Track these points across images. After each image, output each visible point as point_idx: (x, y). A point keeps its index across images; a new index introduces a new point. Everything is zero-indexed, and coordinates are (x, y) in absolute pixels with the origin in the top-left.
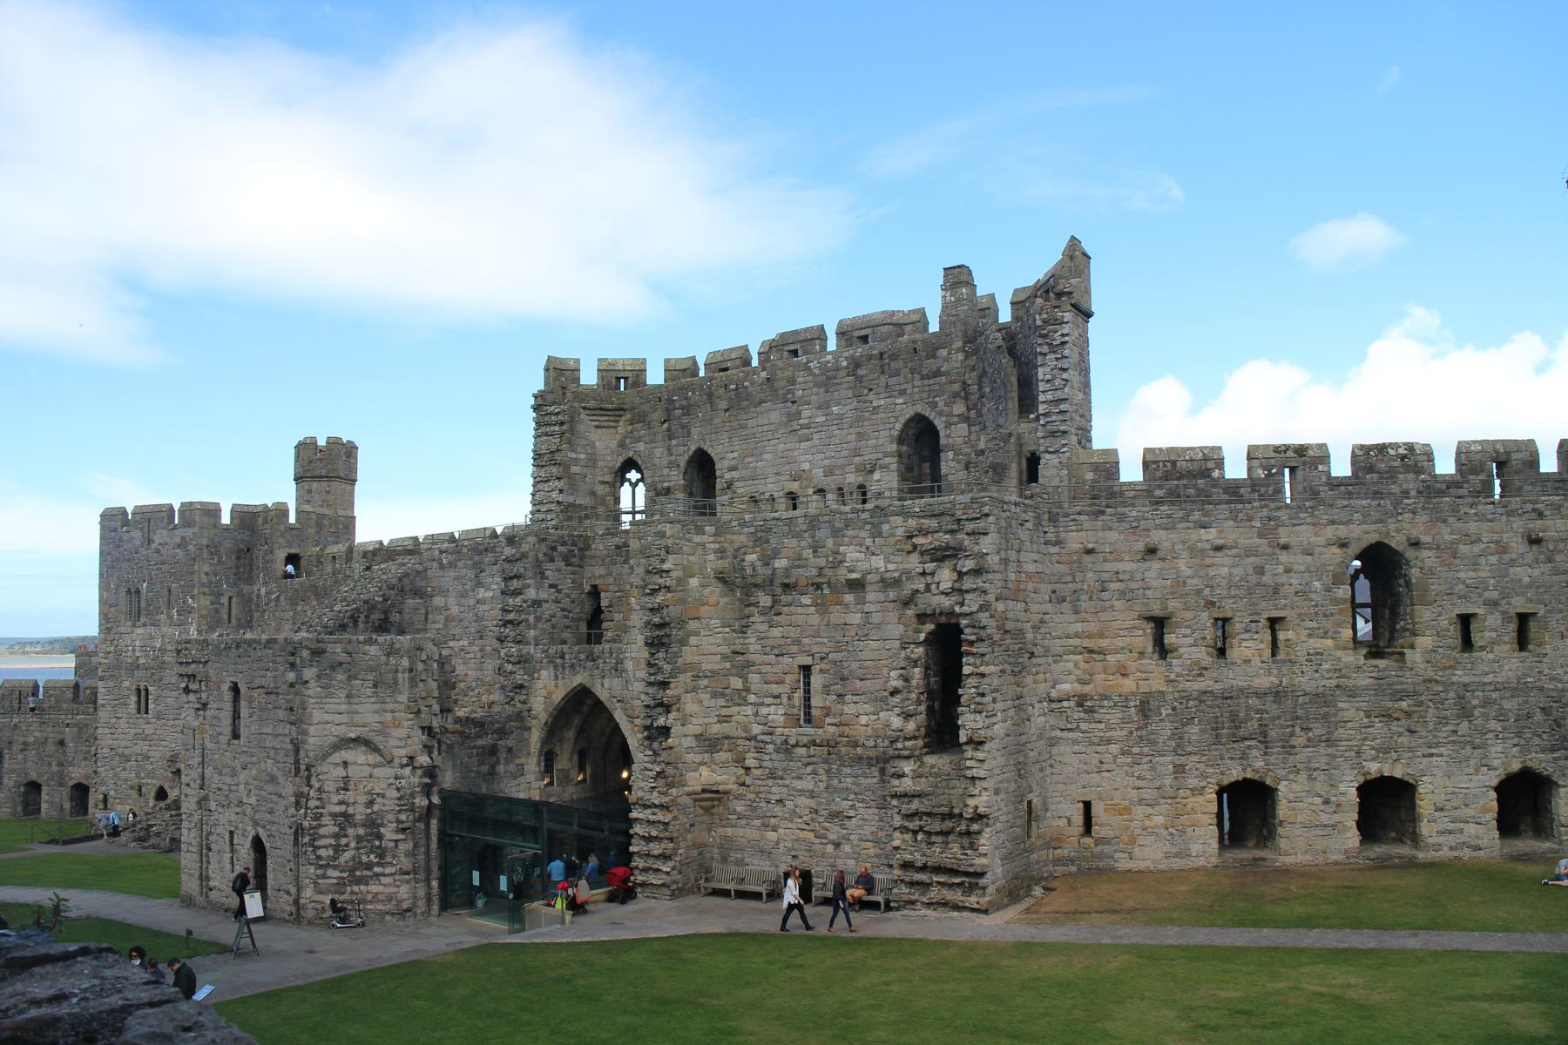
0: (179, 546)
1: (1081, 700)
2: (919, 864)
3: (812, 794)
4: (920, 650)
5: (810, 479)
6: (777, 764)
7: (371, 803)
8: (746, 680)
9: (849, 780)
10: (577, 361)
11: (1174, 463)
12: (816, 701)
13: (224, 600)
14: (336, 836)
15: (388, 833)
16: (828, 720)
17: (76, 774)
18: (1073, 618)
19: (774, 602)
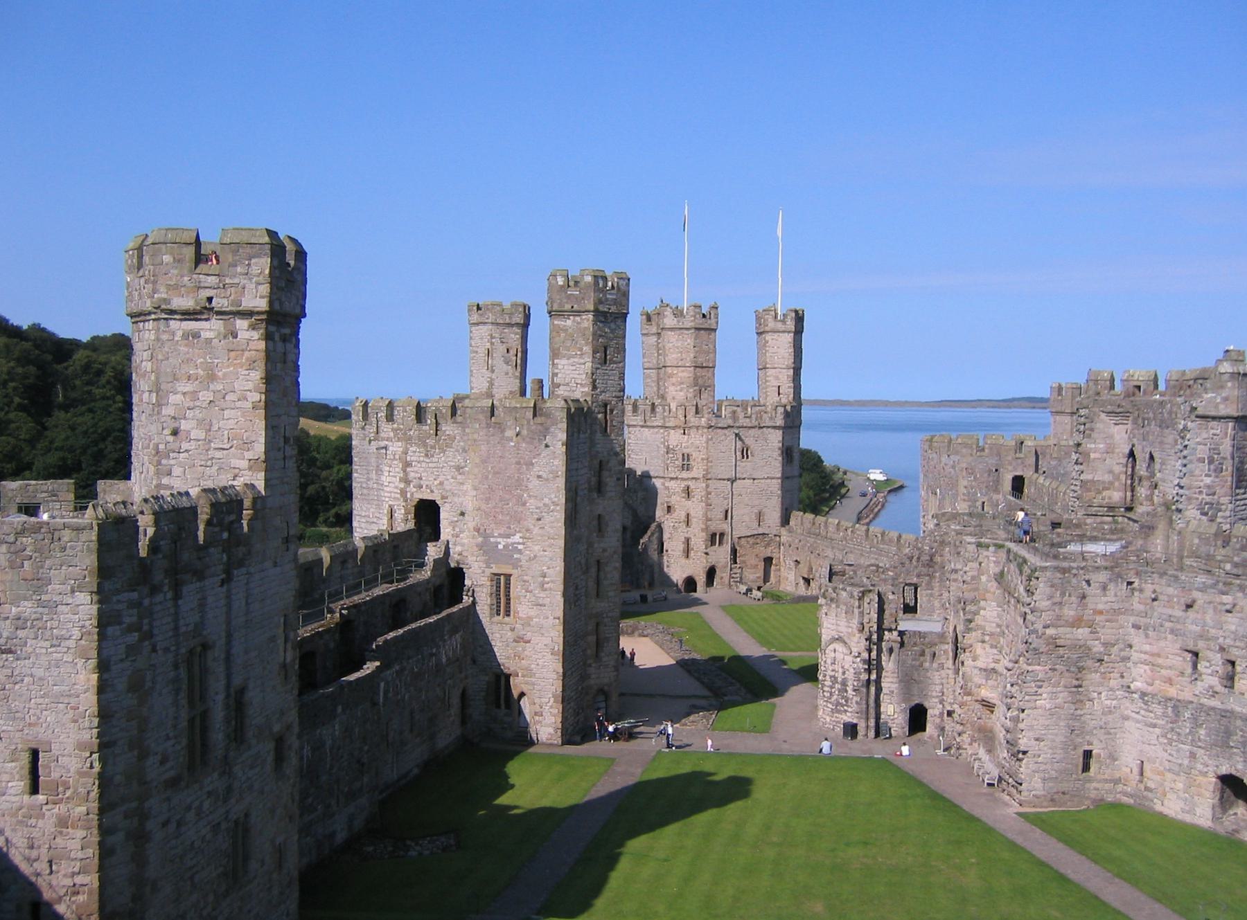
1: (1144, 694)
7: (844, 673)
14: (831, 687)
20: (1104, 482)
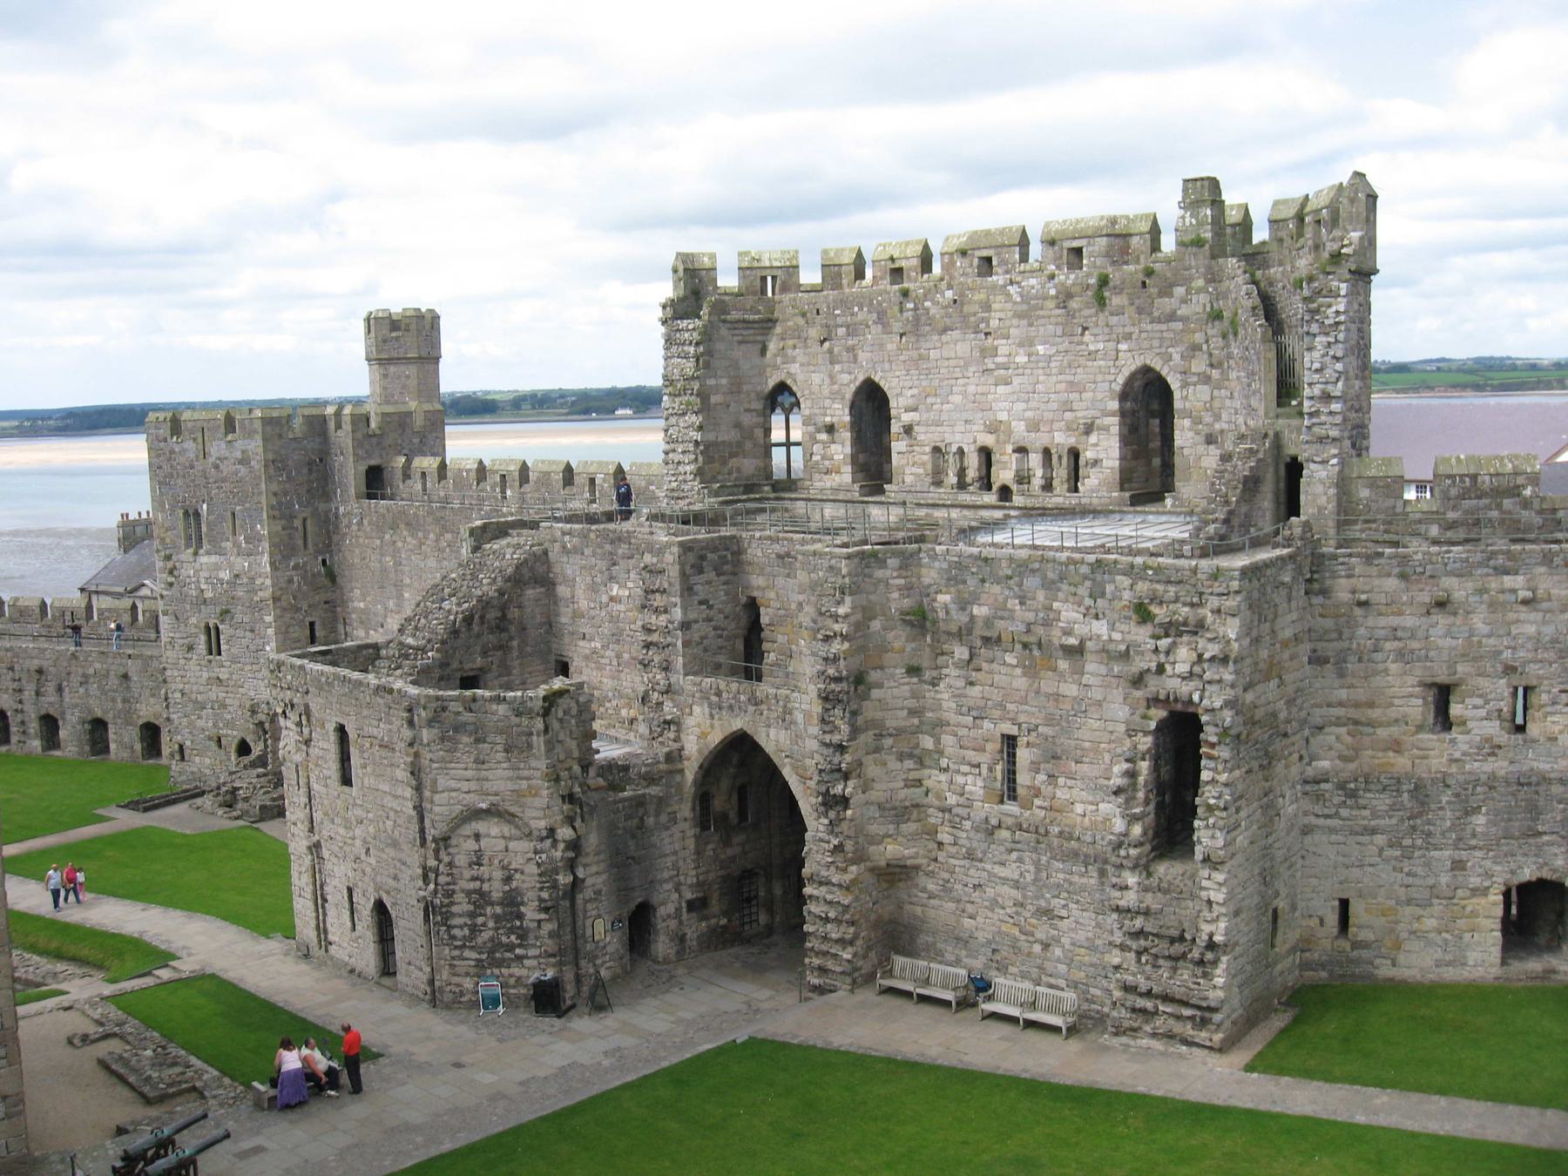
0: (241, 462)
2: (1143, 989)
3: (1016, 885)
4: (1149, 739)
5: (1010, 432)
6: (975, 844)
7: (508, 880)
8: (938, 741)
9: (1061, 876)
10: (713, 256)
11: (1474, 477)
12: (1022, 778)
13: (297, 523)
14: (472, 915)
15: (530, 913)
16: (1037, 802)
17: (148, 710)
18: (1337, 683)
19: (972, 656)
20: (730, 444)
